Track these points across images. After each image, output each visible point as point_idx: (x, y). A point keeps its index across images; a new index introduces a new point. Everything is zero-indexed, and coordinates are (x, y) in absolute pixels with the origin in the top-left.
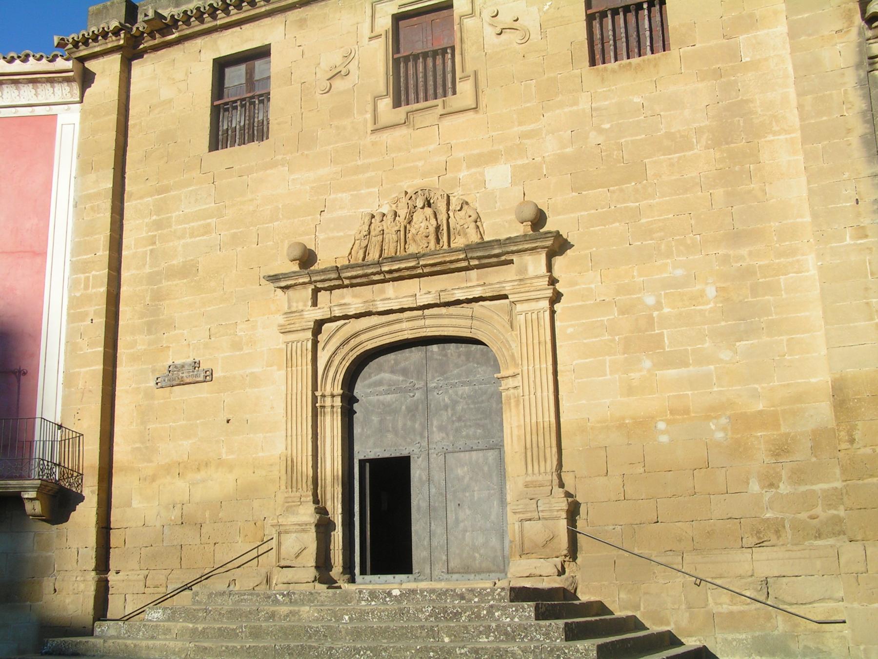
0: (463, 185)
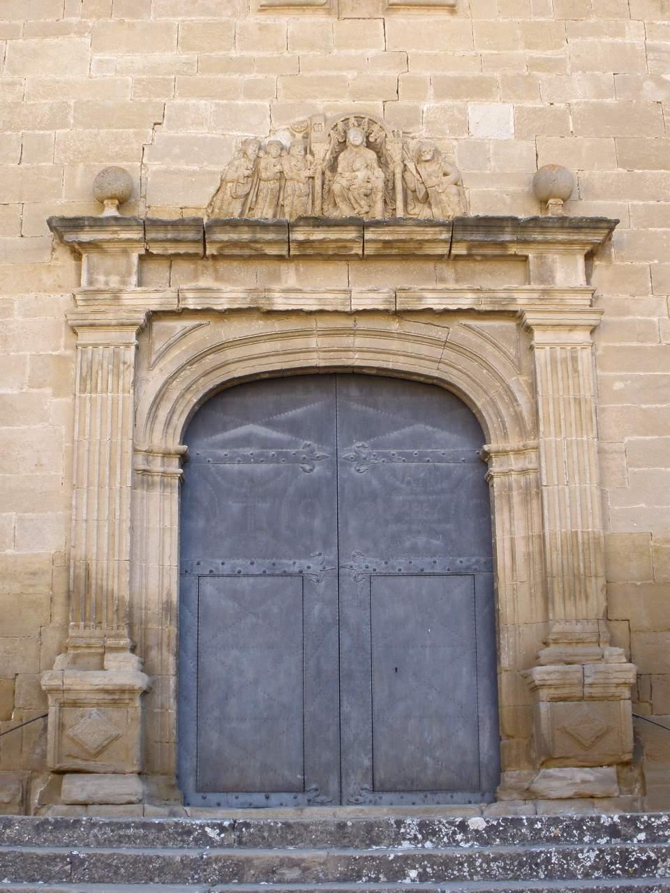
0: (428, 123)
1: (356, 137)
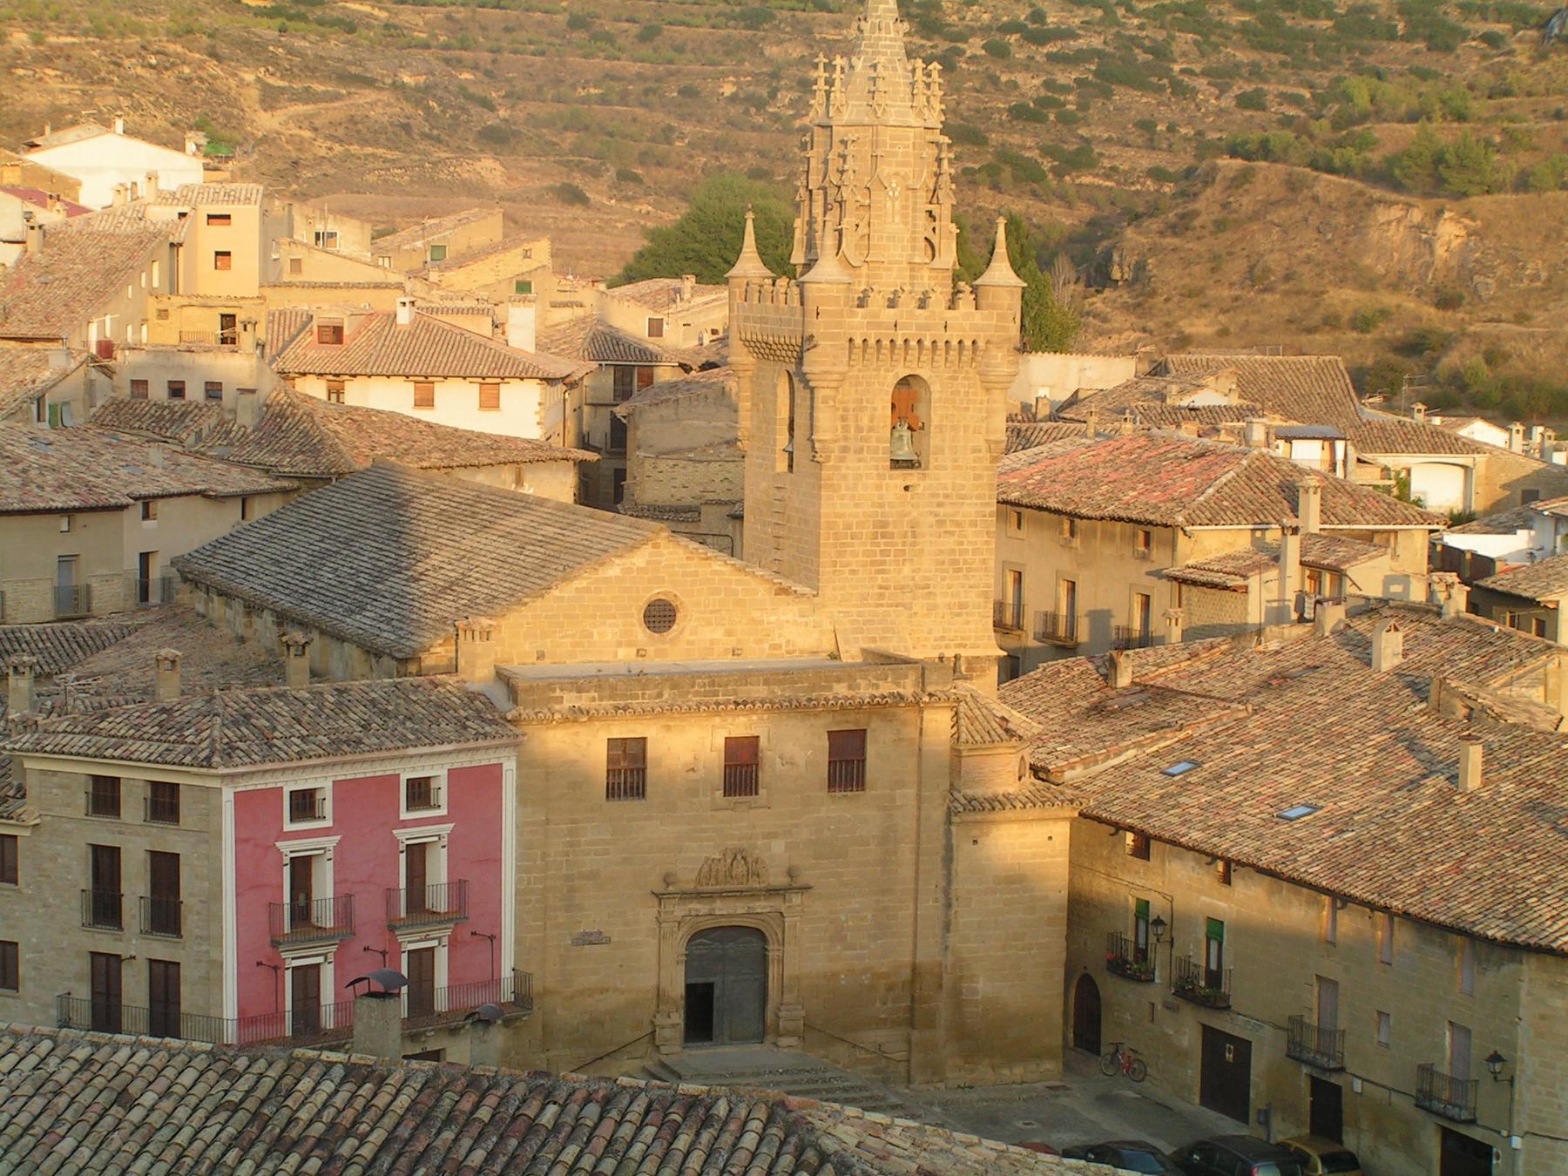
1: (739, 857)
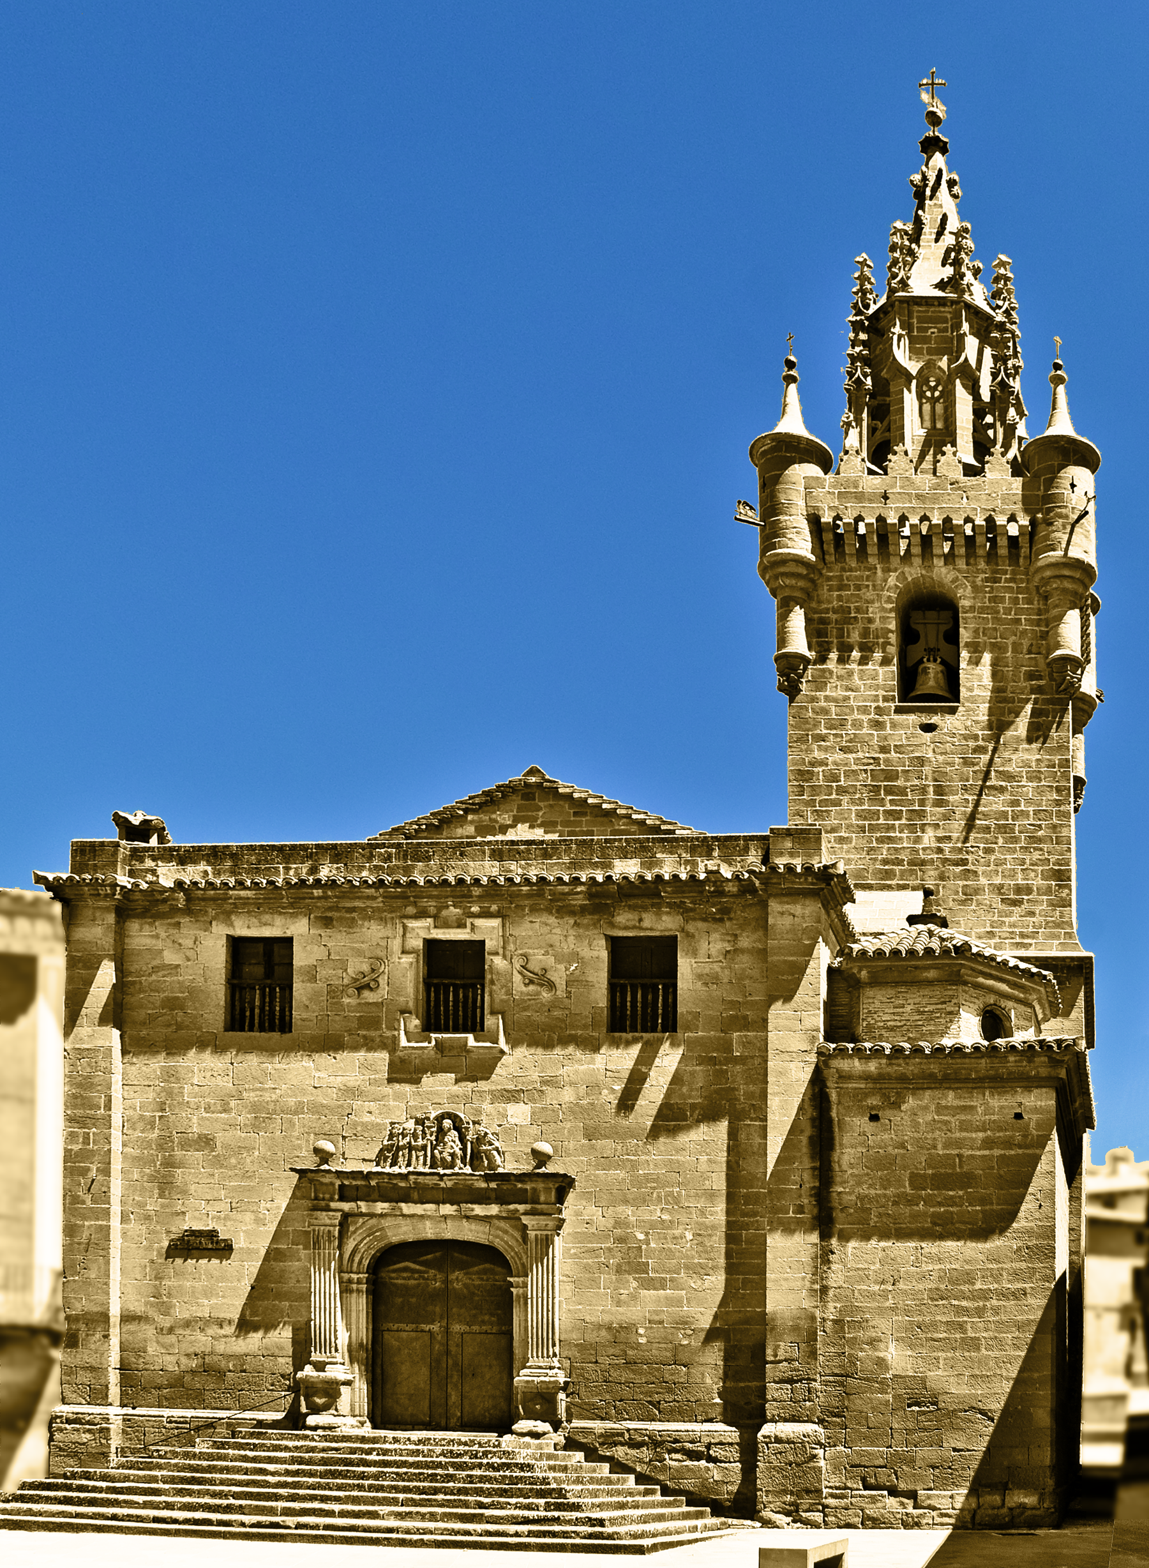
1: (447, 1123)
